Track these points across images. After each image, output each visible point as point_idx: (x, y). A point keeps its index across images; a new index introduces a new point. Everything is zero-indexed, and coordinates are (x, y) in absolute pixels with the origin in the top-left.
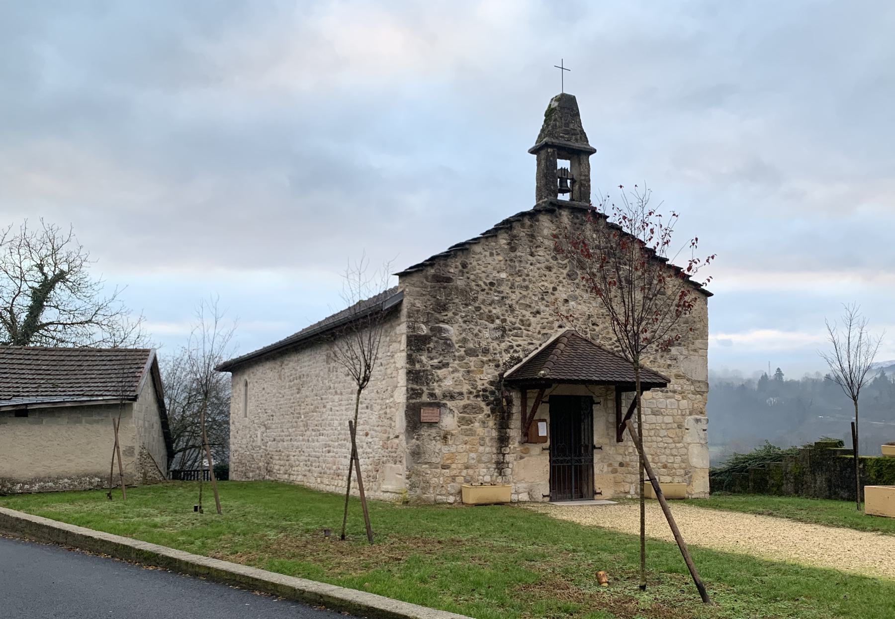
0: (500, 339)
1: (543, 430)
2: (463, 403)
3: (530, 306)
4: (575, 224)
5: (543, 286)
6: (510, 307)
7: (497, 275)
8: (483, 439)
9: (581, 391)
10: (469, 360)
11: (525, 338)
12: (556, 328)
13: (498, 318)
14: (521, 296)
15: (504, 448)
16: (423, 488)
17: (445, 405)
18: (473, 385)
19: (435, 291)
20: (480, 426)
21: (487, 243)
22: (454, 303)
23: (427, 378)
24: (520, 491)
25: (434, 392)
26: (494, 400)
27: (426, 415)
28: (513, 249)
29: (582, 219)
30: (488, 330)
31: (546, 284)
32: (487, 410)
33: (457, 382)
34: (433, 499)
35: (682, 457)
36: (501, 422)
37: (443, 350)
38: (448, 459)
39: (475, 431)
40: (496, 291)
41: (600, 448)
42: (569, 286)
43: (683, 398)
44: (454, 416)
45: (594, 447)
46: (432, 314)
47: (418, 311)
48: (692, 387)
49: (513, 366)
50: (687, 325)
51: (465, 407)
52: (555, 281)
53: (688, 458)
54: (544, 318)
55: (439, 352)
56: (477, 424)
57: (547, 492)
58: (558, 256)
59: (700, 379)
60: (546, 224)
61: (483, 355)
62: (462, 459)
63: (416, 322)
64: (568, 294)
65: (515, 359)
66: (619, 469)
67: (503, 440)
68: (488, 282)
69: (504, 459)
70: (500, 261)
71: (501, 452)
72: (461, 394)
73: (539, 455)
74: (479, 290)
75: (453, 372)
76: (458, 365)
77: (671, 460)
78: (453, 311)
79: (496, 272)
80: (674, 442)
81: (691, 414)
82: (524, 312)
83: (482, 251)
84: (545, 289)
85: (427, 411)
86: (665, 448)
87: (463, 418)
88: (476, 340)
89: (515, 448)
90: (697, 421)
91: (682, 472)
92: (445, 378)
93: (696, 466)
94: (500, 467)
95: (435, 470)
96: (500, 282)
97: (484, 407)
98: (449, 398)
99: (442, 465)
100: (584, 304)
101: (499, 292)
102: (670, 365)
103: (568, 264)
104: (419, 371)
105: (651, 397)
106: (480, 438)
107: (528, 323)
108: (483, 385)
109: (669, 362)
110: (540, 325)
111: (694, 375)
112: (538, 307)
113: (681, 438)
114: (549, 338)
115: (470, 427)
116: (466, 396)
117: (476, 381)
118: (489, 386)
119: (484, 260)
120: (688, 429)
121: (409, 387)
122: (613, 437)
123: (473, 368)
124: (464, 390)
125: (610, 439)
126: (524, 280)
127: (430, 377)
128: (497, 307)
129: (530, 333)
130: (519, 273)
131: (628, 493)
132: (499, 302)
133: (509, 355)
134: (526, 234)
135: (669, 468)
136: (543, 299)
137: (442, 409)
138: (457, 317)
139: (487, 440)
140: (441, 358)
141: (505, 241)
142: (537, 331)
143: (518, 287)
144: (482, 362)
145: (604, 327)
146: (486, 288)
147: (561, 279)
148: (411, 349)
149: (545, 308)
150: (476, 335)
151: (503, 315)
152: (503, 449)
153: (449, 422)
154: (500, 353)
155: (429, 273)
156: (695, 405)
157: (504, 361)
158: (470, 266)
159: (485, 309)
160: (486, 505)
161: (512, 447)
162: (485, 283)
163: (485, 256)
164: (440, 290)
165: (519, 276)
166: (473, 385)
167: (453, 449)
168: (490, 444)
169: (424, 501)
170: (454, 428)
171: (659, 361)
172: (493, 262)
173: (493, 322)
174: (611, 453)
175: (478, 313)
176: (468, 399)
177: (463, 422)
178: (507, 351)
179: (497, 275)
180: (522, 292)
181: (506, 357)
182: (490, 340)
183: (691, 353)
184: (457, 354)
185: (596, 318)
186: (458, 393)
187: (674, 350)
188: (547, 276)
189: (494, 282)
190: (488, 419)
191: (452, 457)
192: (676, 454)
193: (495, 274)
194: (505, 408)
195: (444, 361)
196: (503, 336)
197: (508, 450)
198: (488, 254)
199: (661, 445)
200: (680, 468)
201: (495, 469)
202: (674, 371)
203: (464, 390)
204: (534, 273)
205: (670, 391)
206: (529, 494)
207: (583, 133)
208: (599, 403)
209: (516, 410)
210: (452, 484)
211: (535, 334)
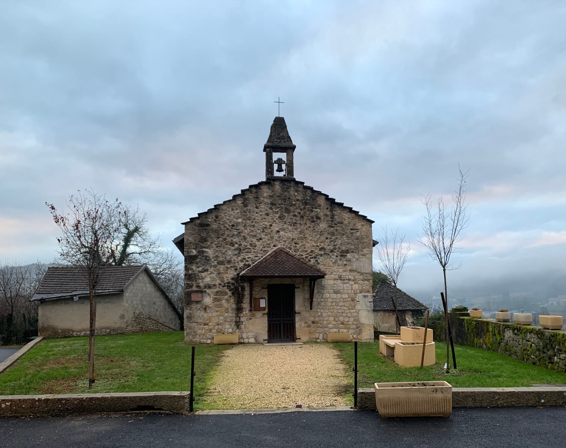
1: (263, 303)
2: (215, 290)
3: (256, 236)
4: (284, 188)
5: (264, 224)
6: (244, 237)
7: (236, 220)
8: (227, 309)
9: (287, 281)
10: (219, 267)
11: (253, 254)
13: (236, 243)
14: (250, 231)
16: (193, 335)
17: (205, 292)
18: (222, 280)
19: (200, 232)
20: (226, 302)
21: (230, 204)
22: (211, 237)
23: (195, 278)
24: (250, 337)
25: (199, 285)
26: (234, 288)
27: (194, 297)
28: (246, 206)
29: (288, 185)
30: (230, 250)
31: (266, 223)
32: (230, 293)
33: (213, 279)
34: (199, 341)
35: (355, 318)
36: (238, 300)
37: (204, 262)
38: (207, 320)
39: (223, 305)
40: (235, 229)
41: (299, 313)
43: (355, 283)
44: (210, 297)
45: (296, 313)
46: (198, 244)
47: (190, 243)
48: (361, 277)
49: (245, 269)
50: (358, 240)
51: (217, 292)
52: (271, 221)
53: (358, 319)
55: (202, 264)
56: (224, 301)
58: (273, 207)
59: (367, 272)
60: (265, 191)
62: (215, 320)
63: (189, 248)
64: (279, 227)
65: (247, 265)
66: (312, 325)
67: (239, 310)
68: (231, 224)
69: (240, 320)
70: (238, 213)
71: (237, 316)
72: (215, 285)
73: (261, 317)
74: (226, 229)
75: (210, 274)
76: (213, 270)
77: (347, 319)
78: (211, 241)
79: (235, 219)
80: (349, 309)
81: (361, 292)
82: (252, 239)
83: (227, 208)
85: (194, 295)
86: (343, 313)
87: (216, 298)
88: (224, 256)
90: (365, 296)
91: (355, 326)
92: (206, 277)
93: (364, 323)
94: (238, 324)
95: (200, 326)
96: (238, 224)
97: (228, 292)
98: (207, 288)
99: (204, 324)
101: (237, 230)
102: (346, 265)
103: (279, 211)
104: (191, 274)
106: (225, 309)
107: (254, 245)
108: (228, 280)
109: (345, 263)
110: (262, 246)
111: (362, 270)
112: (260, 236)
113: (354, 307)
114: (268, 252)
115: (220, 303)
116: (218, 286)
117: (223, 278)
118: (231, 281)
119: (228, 213)
120: (359, 302)
121: (186, 283)
122: (308, 307)
123: (222, 271)
124: (217, 283)
125: (306, 308)
126: (252, 222)
127: (197, 277)
128: (236, 237)
129: (256, 251)
130: (249, 219)
131: (318, 338)
132: (237, 235)
133: (243, 263)
134: (253, 197)
135: (345, 324)
136: (263, 231)
137: (204, 294)
138: (213, 244)
139: (230, 309)
140: (204, 267)
141: (241, 202)
142: (260, 249)
145: (302, 245)
146: (230, 228)
147: (275, 219)
148: (186, 263)
149: (265, 236)
150: (224, 253)
151: (239, 242)
152: (239, 315)
153: (208, 300)
154: (238, 262)
155: (196, 223)
156: (364, 287)
157: (240, 267)
158: (220, 217)
159: (229, 239)
160: (225, 344)
161: (244, 313)
162: (229, 225)
163: (229, 211)
164: (203, 231)
165: (249, 220)
166: (222, 280)
167: (210, 315)
168: (231, 312)
169: (194, 342)
170: (210, 303)
171: (339, 262)
172: (234, 214)
173: (233, 246)
174: (307, 316)
175: (225, 242)
176: (219, 288)
177: (216, 301)
178: (242, 261)
179: (236, 220)
180: (251, 228)
181: (242, 264)
182: (232, 256)
183: (361, 256)
184: (213, 264)
185: (297, 239)
186: (213, 285)
187: (349, 256)
188: (266, 219)
189: (234, 224)
190: (230, 298)
191: (210, 319)
192: (351, 316)
193: (235, 220)
194: (240, 292)
195: (205, 268)
196: (239, 253)
197: (242, 315)
198: (230, 209)
199: (340, 311)
200: (353, 324)
201: (235, 325)
202: (349, 268)
203: (217, 283)
204: (258, 217)
205: (346, 279)
206: (255, 339)
207: (289, 137)
208: (299, 288)
209: (247, 293)
210: (210, 333)
211: (259, 251)
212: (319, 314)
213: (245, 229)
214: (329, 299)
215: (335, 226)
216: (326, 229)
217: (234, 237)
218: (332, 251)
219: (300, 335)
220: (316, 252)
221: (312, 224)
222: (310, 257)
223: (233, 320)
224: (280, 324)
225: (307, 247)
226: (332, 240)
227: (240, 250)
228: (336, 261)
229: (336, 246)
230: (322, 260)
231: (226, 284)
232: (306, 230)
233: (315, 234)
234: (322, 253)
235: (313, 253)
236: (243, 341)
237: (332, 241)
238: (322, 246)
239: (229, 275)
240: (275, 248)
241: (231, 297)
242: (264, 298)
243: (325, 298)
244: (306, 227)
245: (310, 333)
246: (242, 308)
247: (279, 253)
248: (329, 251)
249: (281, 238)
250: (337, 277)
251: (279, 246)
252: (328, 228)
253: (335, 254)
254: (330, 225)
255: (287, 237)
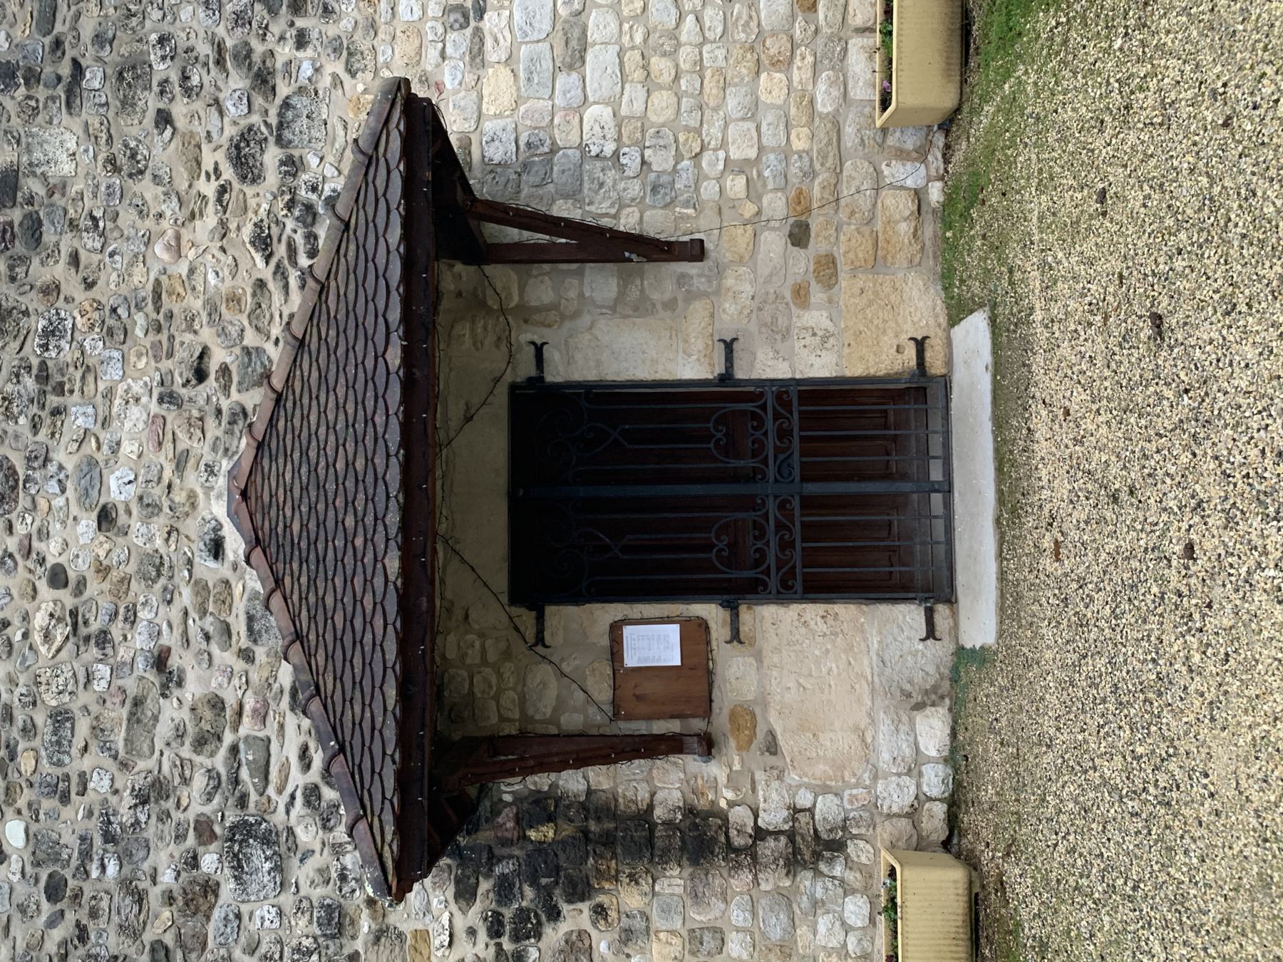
0: (283, 849)
3: (138, 703)
5: (47, 637)
6: (144, 801)
11: (271, 730)
12: (224, 570)
15: (733, 833)
20: (642, 951)
24: (908, 751)
26: (534, 883)
30: (245, 909)
31: (40, 620)
32: (576, 917)
41: (729, 346)
42: (42, 503)
45: (726, 378)
54: (185, 632)
57: (909, 616)
61: (349, 931)
64: (74, 510)
66: (818, 245)
68: (46, 907)
69: (777, 834)
73: (759, 657)
74: (81, 951)
82: (164, 730)
84: (60, 620)
89: (732, 782)
97: (564, 927)
100: (116, 424)
101: (86, 855)
105: (505, 73)
107: (208, 714)
108: (472, 932)
110: (215, 649)
112: (140, 664)
118: (477, 907)
122: (682, 279)
125: (691, 296)
126: (29, 730)
128: (146, 866)
129: (250, 703)
136: (103, 639)
139: (699, 917)
142: (239, 665)
143: (60, 764)
144: (377, 940)
145: (211, 322)
146: (70, 917)
149: (141, 626)
151: (180, 837)
152: (738, 841)
161: (730, 795)
162: (52, 923)
171: (346, 24)
173: (210, 888)
174: (748, 289)
180: (78, 743)
182: (287, 900)
190: (613, 914)
194: (568, 830)
196: (267, 840)
197: (740, 816)
201: (818, 873)
206: (919, 707)
208: (539, 350)
211: (254, 677)
212: (736, 185)
213: (82, 793)
214: (624, 111)
215: (70, 53)
216: (95, 122)
217: (144, 884)
218: (263, 80)
219: (889, 342)
220: (265, 206)
221: (49, 236)
222: (304, 261)
223: (778, 891)
224: (809, 503)
225: (229, 282)
226: (174, 77)
227: (243, 833)
228: (337, 51)
229: (220, 48)
230: (330, 158)
231: (508, 946)
232: (95, 293)
233: (127, 217)
234: (272, 157)
235: (275, 231)
236: (940, 810)
237: (185, 78)
238: (220, 156)
239: (436, 919)
240: (235, 544)
241: (600, 912)
242: (615, 631)
243: (618, 139)
244: (72, 285)
245: (877, 261)
246: (690, 811)
247: (259, 517)
248: (259, 101)
249: (157, 492)
250: (459, 41)
251: (219, 509)
252: (89, 114)
253: (285, 52)
254: (60, 91)
255: (150, 448)
